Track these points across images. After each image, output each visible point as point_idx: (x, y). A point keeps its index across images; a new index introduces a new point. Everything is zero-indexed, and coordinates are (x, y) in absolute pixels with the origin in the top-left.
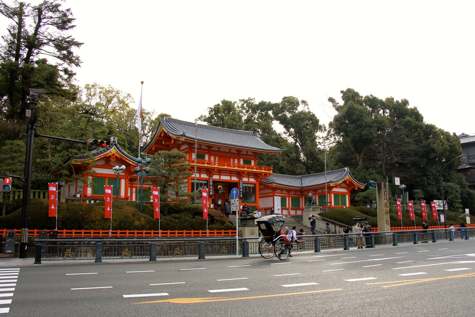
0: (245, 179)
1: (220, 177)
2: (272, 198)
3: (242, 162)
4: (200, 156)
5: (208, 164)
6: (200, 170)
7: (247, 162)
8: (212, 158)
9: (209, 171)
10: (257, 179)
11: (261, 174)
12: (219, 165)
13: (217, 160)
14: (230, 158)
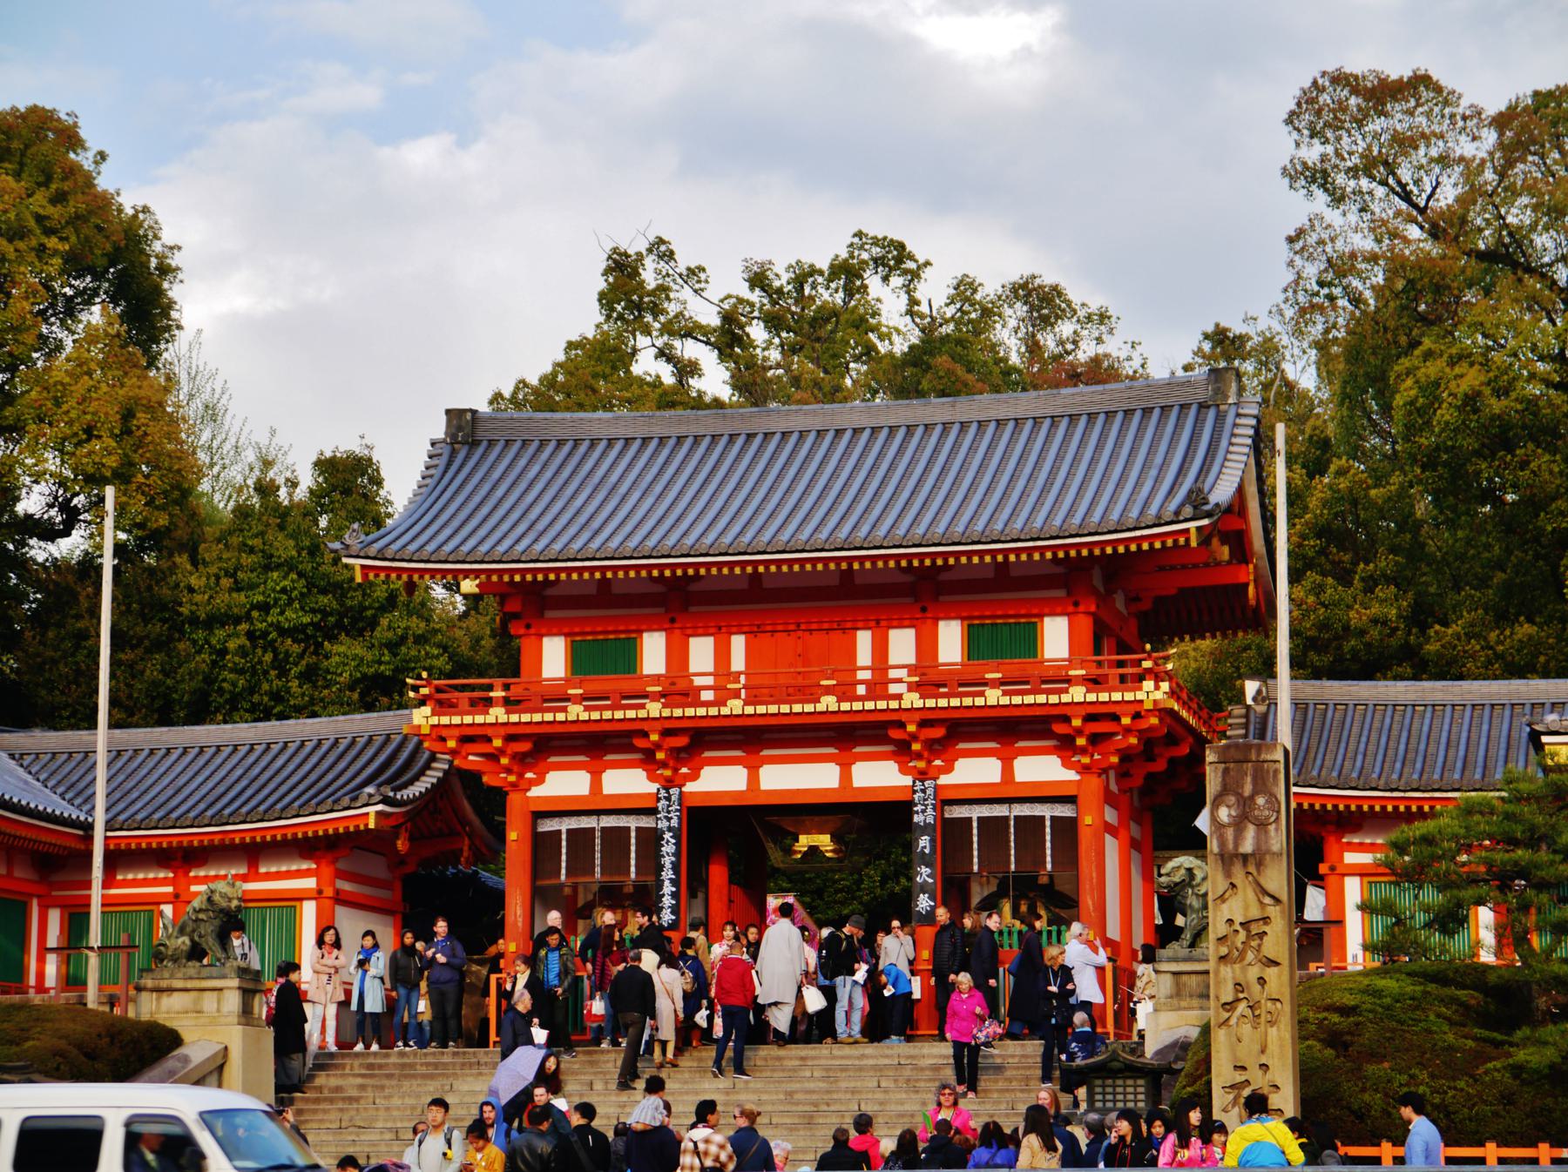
0: (975, 770)
3: (951, 640)
4: (603, 658)
5: (667, 697)
6: (596, 746)
13: (738, 662)
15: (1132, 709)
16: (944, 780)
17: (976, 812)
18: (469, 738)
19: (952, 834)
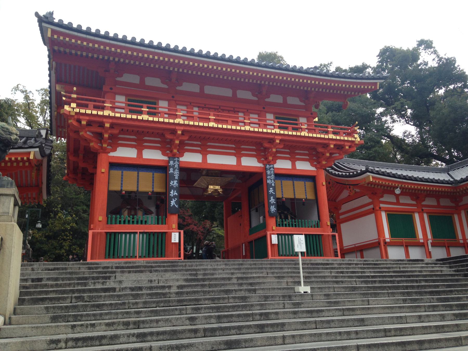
1: (205, 159)
2: (373, 216)
9: (165, 138)
10: (319, 163)
11: (325, 144)
14: (236, 112)
15: (349, 144)
16: (276, 166)
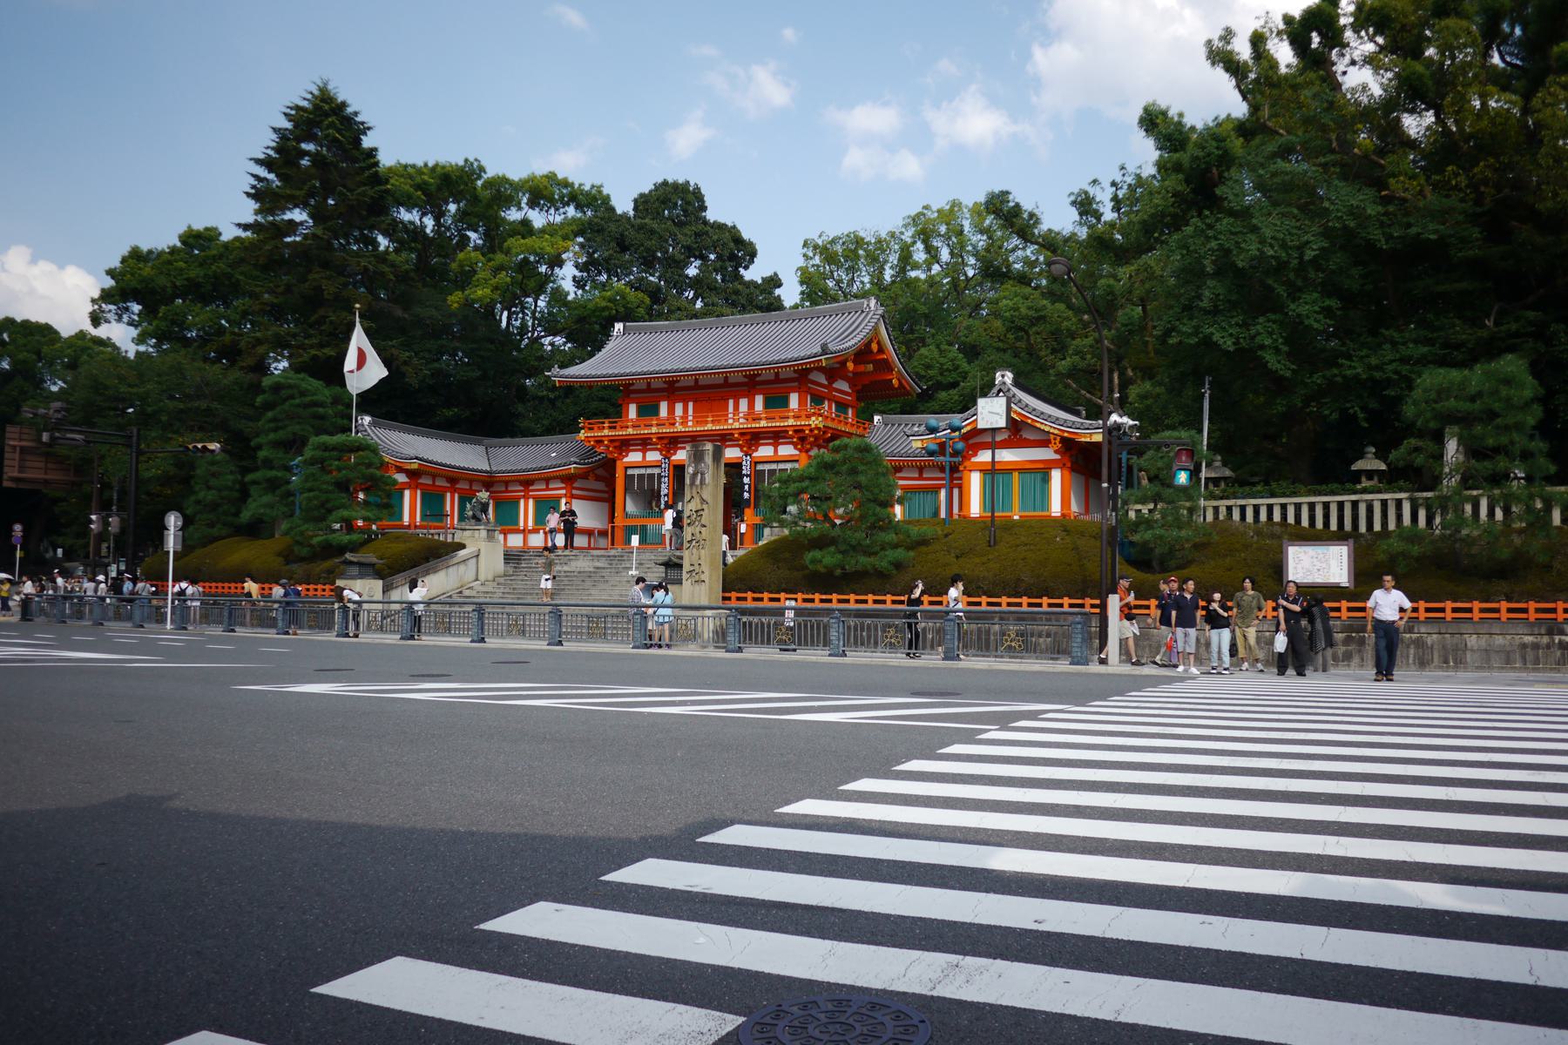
0: (765, 451)
3: (759, 402)
4: (648, 410)
6: (644, 444)
7: (776, 401)
8: (679, 408)
12: (698, 423)
17: (767, 467)
18: (599, 442)
19: (758, 476)
